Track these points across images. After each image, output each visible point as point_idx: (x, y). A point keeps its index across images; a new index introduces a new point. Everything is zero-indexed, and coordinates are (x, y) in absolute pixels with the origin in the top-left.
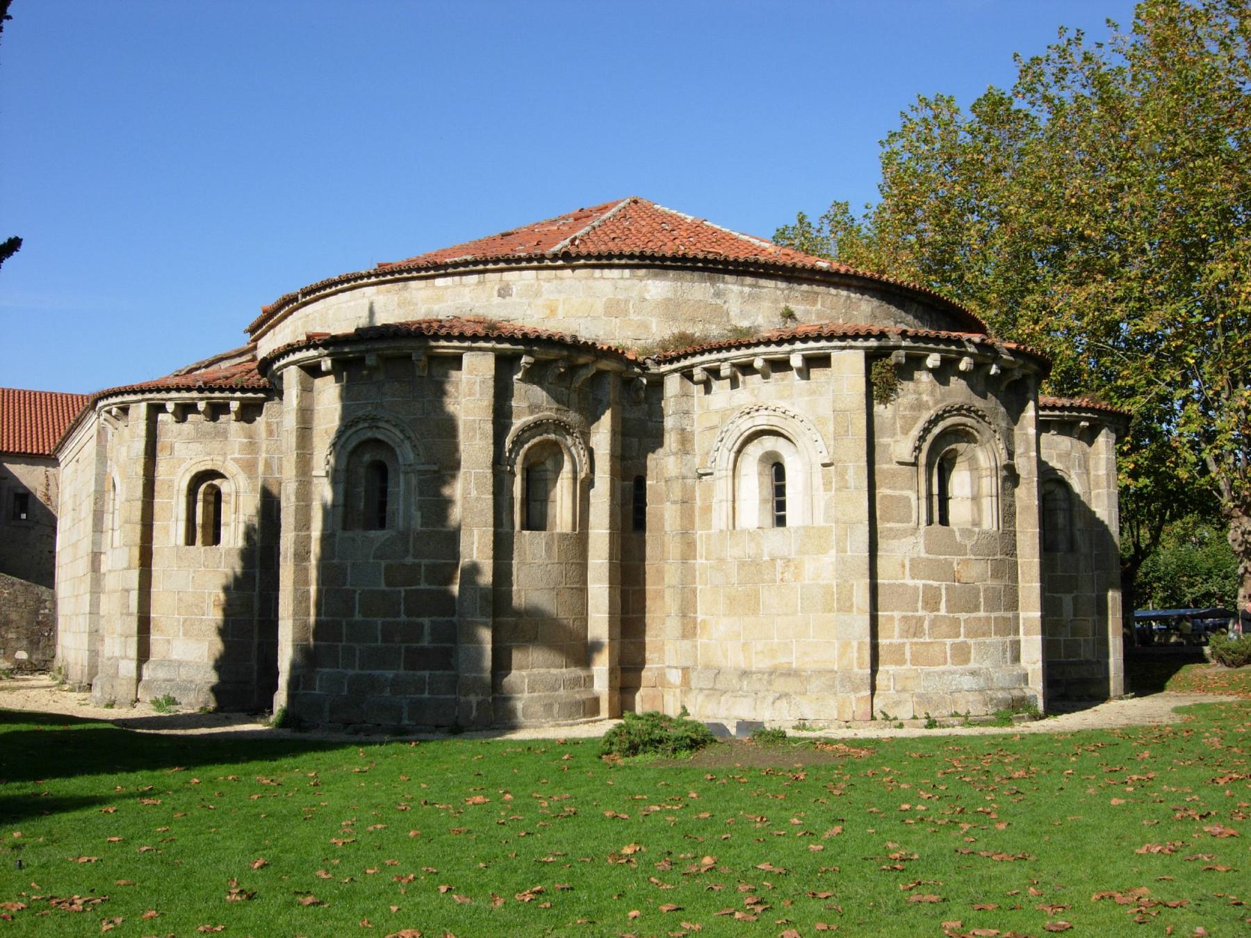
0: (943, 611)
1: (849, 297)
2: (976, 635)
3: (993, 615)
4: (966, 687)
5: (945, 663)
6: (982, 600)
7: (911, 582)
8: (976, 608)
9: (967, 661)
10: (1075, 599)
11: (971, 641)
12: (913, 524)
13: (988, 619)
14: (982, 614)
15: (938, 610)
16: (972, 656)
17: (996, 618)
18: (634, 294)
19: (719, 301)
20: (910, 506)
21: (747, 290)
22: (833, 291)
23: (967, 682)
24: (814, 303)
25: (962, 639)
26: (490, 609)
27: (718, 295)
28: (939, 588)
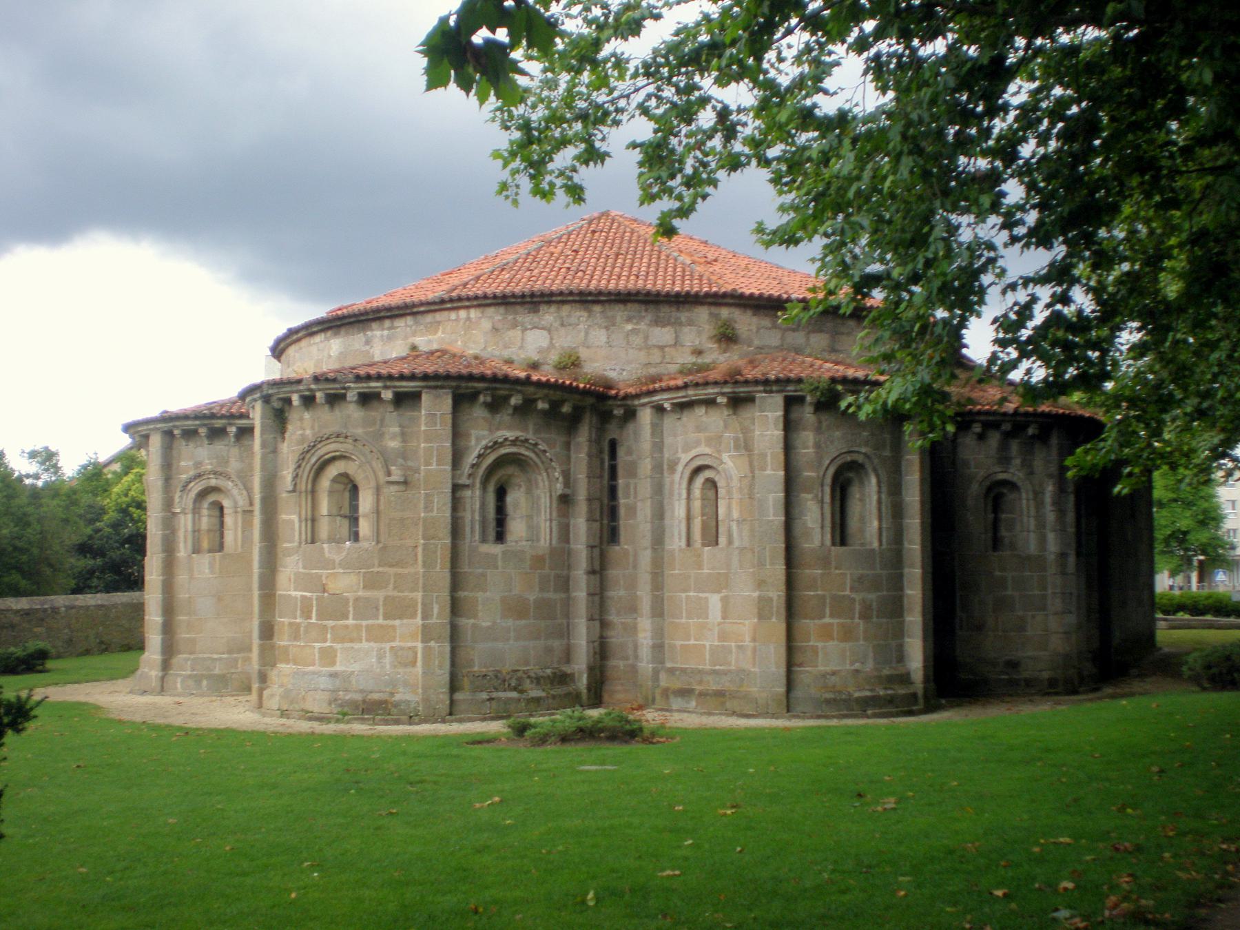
0: (313, 620)
1: (468, 319)
2: (342, 641)
3: (364, 623)
4: (322, 687)
5: (314, 665)
6: (351, 609)
7: (293, 593)
8: (345, 616)
9: (333, 663)
10: (725, 600)
11: (338, 646)
12: (296, 544)
13: (358, 627)
14: (351, 622)
15: (310, 618)
16: (338, 659)
17: (367, 626)
18: (325, 354)
19: (367, 348)
20: (293, 529)
21: (386, 332)
22: (453, 315)
23: (324, 683)
24: (436, 332)
25: (328, 644)
26: (160, 612)
27: (367, 342)
28: (310, 599)
